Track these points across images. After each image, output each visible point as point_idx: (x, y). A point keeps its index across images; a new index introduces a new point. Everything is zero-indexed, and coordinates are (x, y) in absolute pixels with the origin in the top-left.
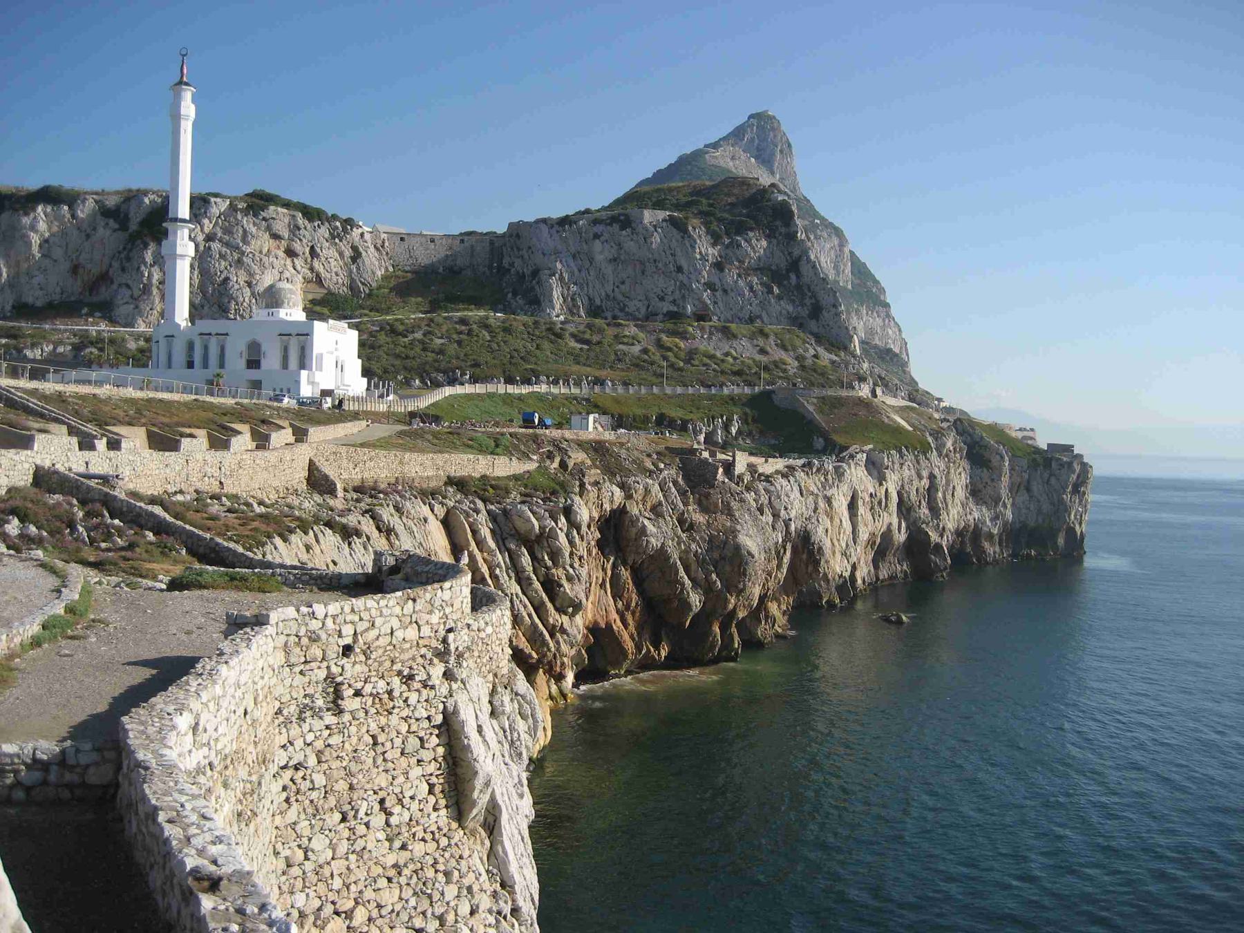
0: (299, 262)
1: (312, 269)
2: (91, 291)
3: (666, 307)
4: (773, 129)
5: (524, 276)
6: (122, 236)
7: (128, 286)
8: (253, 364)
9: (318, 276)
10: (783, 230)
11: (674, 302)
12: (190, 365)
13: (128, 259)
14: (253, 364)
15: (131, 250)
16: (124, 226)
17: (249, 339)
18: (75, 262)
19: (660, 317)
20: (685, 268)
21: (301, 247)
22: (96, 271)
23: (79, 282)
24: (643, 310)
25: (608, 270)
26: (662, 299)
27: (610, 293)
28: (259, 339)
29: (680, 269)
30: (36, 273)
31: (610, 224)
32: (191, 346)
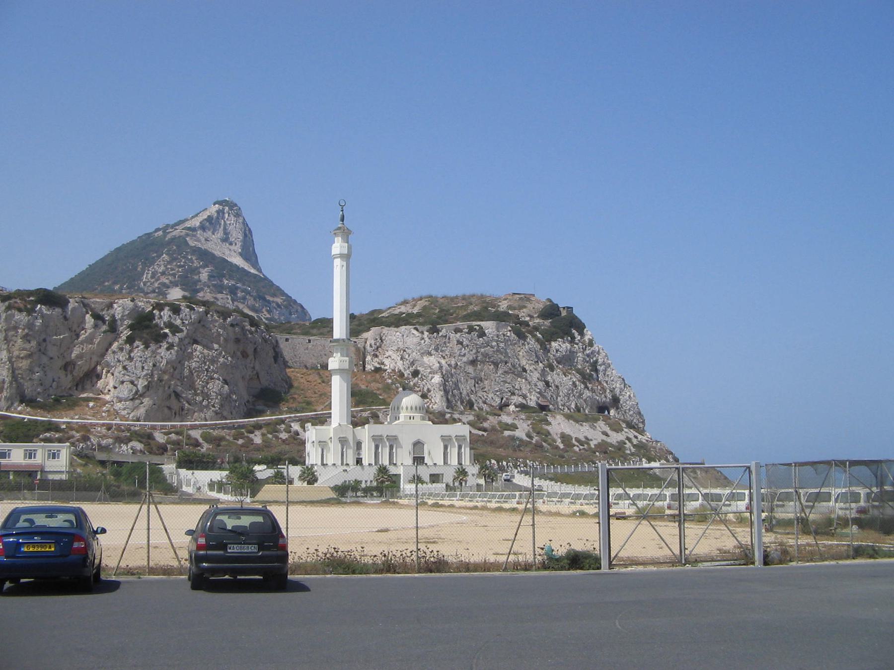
0: (248, 360)
1: (254, 368)
2: (77, 385)
3: (517, 399)
4: (238, 215)
5: (402, 375)
6: (111, 336)
7: (132, 383)
8: (419, 460)
9: (257, 374)
10: (579, 337)
11: (525, 397)
12: (359, 461)
13: (131, 359)
14: (419, 460)
15: (131, 351)
16: (113, 328)
17: (415, 440)
18: (68, 360)
19: (512, 408)
20: (527, 367)
21: (250, 351)
22: (85, 369)
23: (70, 377)
24: (498, 400)
25: (470, 369)
26: (513, 394)
27: (473, 389)
28: (422, 439)
29: (525, 370)
30: (37, 369)
31: (469, 333)
32: (359, 445)
